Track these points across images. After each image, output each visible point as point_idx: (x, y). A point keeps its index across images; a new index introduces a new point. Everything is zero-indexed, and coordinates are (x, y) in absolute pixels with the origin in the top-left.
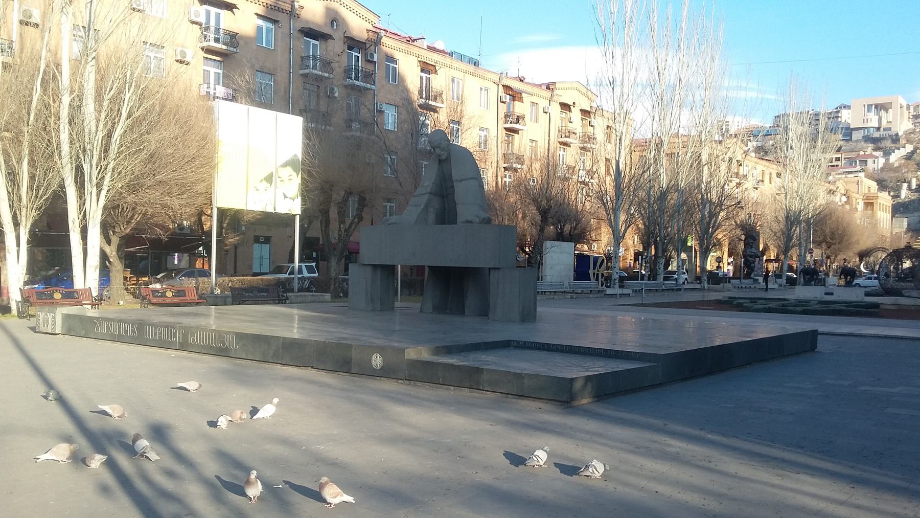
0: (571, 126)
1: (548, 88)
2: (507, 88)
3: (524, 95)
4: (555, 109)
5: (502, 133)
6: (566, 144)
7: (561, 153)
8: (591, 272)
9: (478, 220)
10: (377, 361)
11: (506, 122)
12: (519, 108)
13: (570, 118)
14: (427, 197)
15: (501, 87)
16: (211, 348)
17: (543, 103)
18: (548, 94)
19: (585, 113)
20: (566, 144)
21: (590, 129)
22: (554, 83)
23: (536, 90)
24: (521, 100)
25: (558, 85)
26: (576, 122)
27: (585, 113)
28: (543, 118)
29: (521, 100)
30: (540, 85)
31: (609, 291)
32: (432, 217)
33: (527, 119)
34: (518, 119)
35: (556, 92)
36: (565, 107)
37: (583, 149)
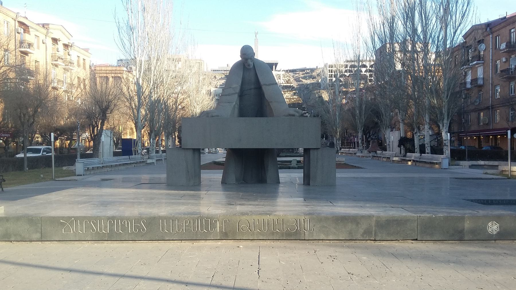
0: (58, 54)
1: (43, 26)
2: (21, 24)
3: (31, 30)
4: (49, 42)
5: (18, 54)
6: (56, 66)
7: (53, 71)
8: (133, 149)
11: (20, 48)
12: (29, 38)
13: (58, 49)
14: (236, 96)
15: (17, 22)
16: (273, 234)
17: (42, 37)
18: (44, 31)
19: (66, 46)
20: (56, 66)
21: (68, 57)
22: (48, 24)
23: (37, 27)
24: (29, 32)
25: (50, 26)
26: (62, 52)
27: (66, 46)
28: (42, 46)
29: (29, 32)
30: (38, 24)
31: (149, 161)
32: (236, 111)
33: (35, 46)
34: (30, 45)
35: (50, 31)
36: (55, 41)
37: (65, 69)
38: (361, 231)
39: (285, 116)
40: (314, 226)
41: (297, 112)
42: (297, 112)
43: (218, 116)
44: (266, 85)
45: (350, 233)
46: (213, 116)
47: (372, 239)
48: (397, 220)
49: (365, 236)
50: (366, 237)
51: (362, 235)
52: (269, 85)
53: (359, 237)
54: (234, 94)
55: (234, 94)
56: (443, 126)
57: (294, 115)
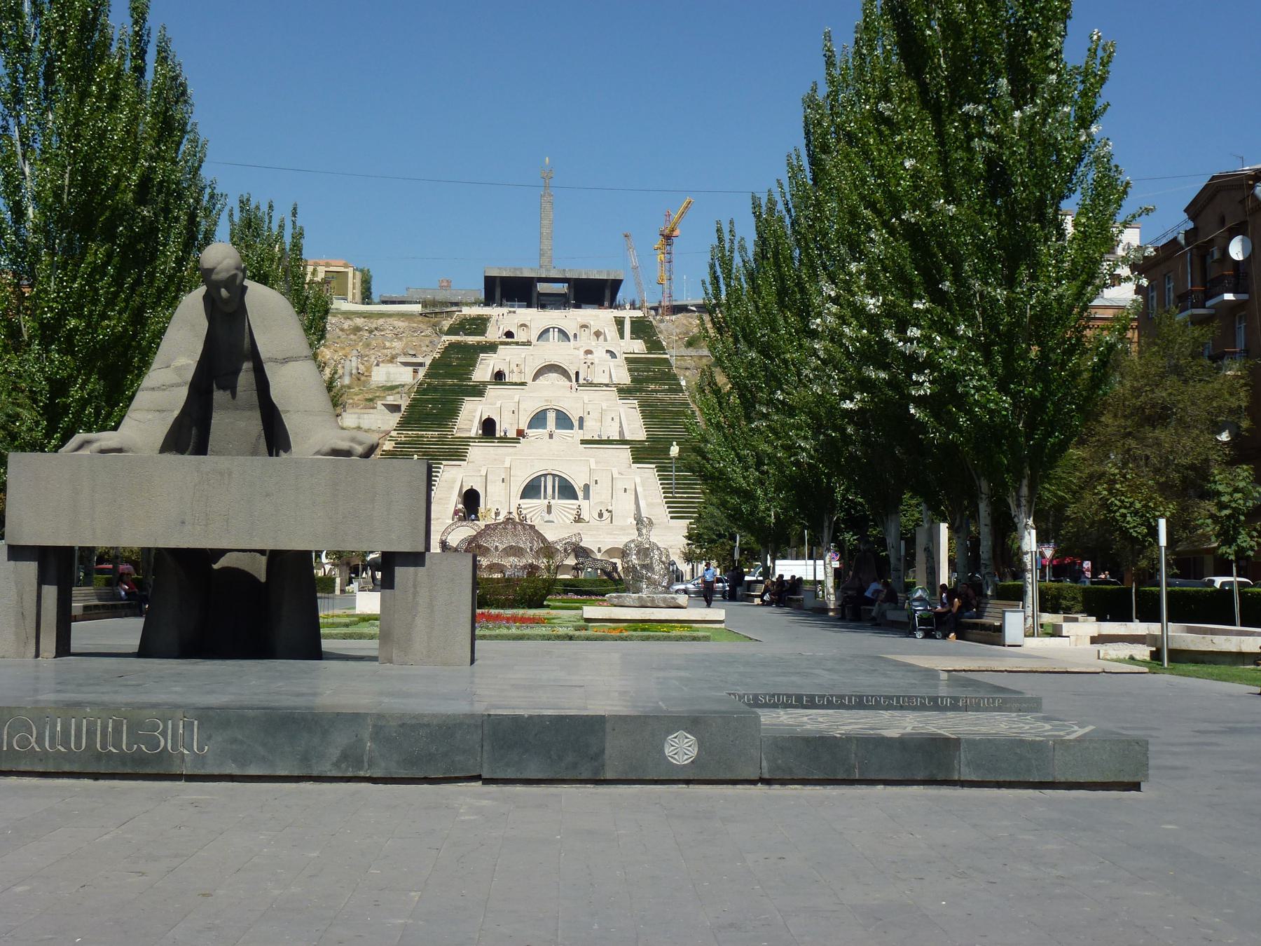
9: (360, 449)
10: (681, 749)
14: (183, 393)
16: (99, 757)
38: (334, 753)
39: (318, 453)
40: (210, 738)
41: (360, 443)
42: (360, 443)
43: (120, 450)
44: (275, 361)
45: (305, 759)
46: (103, 451)
47: (362, 774)
48: (429, 725)
49: (343, 766)
50: (347, 770)
51: (336, 765)
52: (286, 361)
53: (327, 769)
54: (178, 385)
55: (178, 385)
56: (1019, 506)
57: (348, 453)
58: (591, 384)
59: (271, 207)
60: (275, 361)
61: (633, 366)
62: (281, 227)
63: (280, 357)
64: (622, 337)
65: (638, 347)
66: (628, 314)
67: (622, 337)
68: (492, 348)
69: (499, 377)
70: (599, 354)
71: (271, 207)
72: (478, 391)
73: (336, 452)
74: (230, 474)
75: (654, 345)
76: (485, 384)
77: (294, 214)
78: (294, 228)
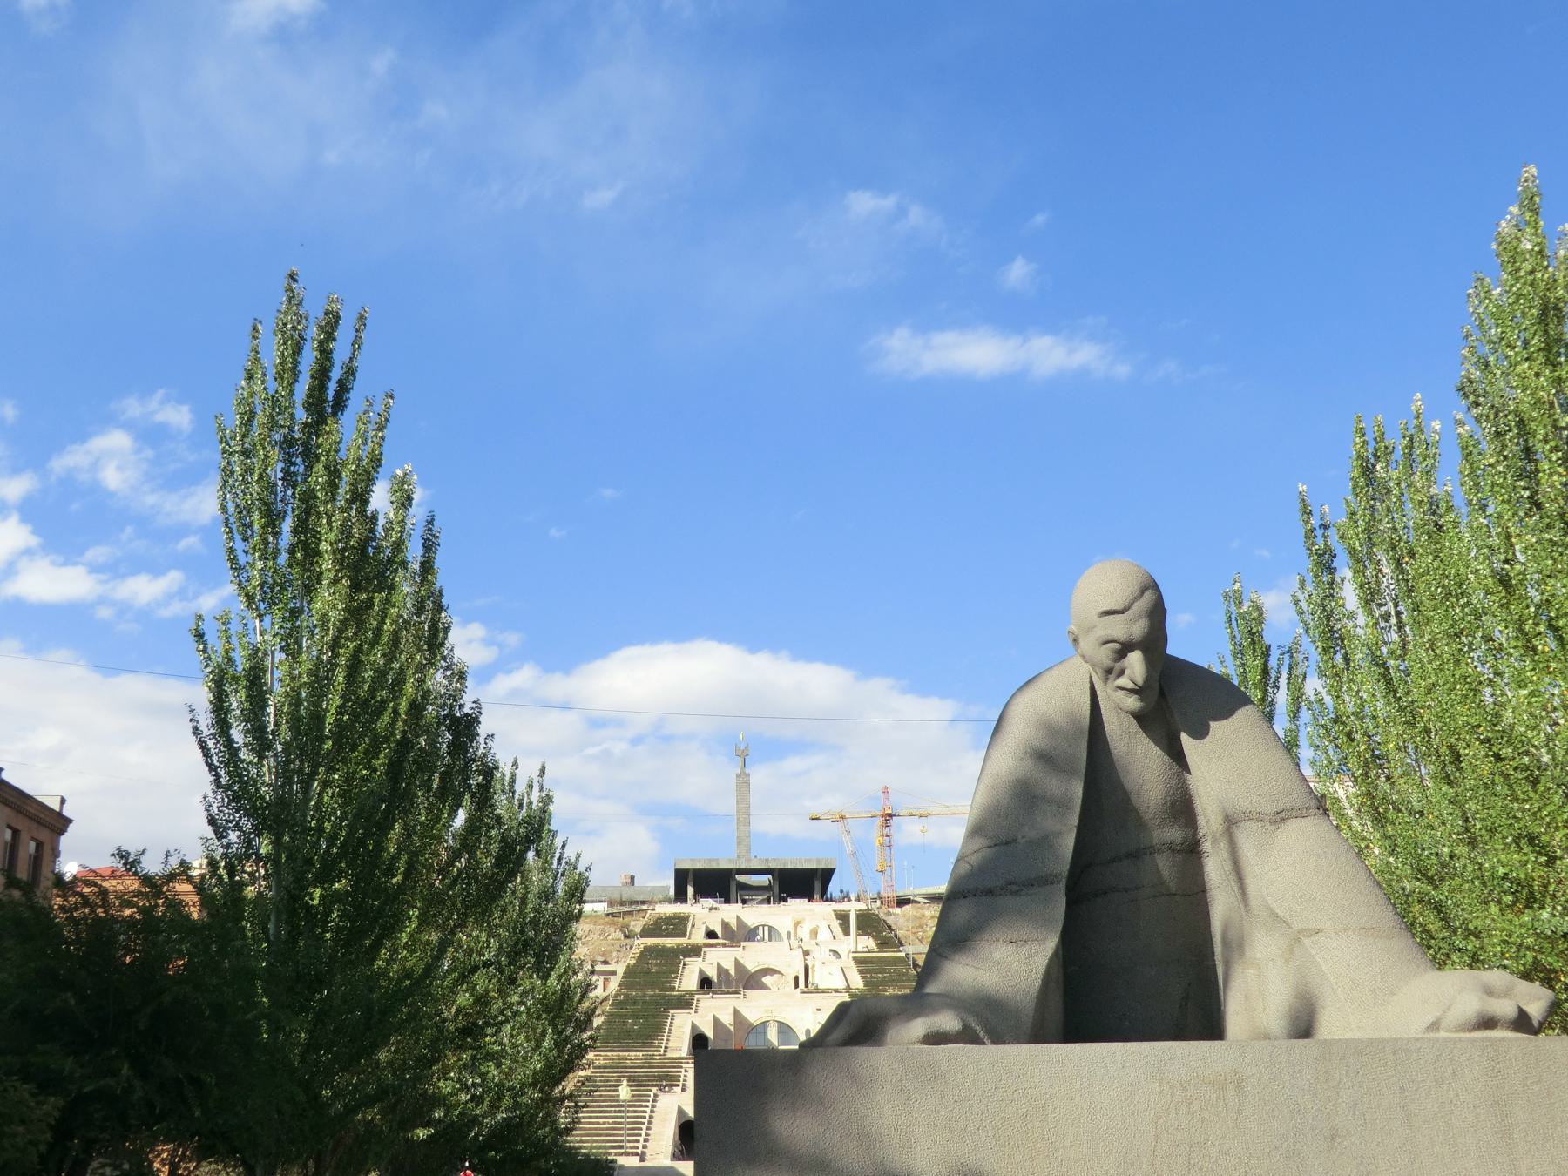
39: (1435, 1026)
44: (1260, 818)
52: (1281, 817)
58: (817, 990)
59: (515, 764)
60: (1260, 818)
61: (863, 967)
62: (530, 787)
63: (1269, 808)
64: (847, 933)
65: (867, 943)
66: (853, 907)
67: (847, 933)
68: (695, 951)
69: (705, 983)
70: (820, 955)
71: (515, 764)
72: (685, 1002)
73: (1488, 1023)
74: (1239, 1085)
75: (884, 944)
76: (691, 994)
77: (542, 772)
78: (541, 790)
